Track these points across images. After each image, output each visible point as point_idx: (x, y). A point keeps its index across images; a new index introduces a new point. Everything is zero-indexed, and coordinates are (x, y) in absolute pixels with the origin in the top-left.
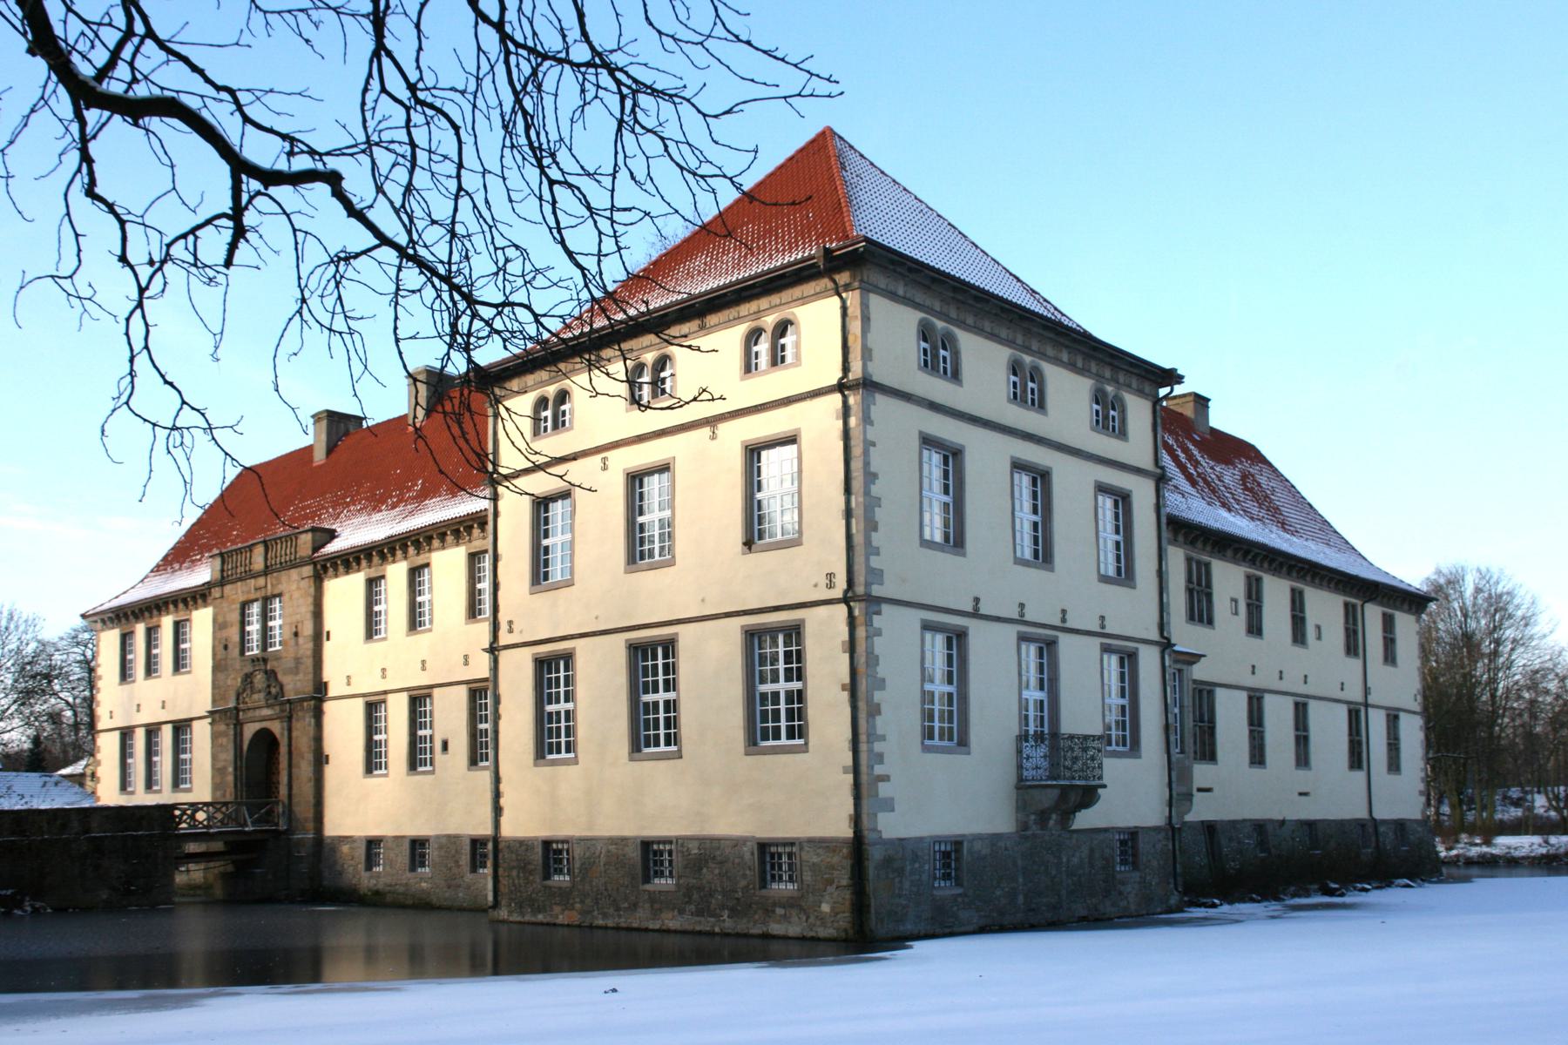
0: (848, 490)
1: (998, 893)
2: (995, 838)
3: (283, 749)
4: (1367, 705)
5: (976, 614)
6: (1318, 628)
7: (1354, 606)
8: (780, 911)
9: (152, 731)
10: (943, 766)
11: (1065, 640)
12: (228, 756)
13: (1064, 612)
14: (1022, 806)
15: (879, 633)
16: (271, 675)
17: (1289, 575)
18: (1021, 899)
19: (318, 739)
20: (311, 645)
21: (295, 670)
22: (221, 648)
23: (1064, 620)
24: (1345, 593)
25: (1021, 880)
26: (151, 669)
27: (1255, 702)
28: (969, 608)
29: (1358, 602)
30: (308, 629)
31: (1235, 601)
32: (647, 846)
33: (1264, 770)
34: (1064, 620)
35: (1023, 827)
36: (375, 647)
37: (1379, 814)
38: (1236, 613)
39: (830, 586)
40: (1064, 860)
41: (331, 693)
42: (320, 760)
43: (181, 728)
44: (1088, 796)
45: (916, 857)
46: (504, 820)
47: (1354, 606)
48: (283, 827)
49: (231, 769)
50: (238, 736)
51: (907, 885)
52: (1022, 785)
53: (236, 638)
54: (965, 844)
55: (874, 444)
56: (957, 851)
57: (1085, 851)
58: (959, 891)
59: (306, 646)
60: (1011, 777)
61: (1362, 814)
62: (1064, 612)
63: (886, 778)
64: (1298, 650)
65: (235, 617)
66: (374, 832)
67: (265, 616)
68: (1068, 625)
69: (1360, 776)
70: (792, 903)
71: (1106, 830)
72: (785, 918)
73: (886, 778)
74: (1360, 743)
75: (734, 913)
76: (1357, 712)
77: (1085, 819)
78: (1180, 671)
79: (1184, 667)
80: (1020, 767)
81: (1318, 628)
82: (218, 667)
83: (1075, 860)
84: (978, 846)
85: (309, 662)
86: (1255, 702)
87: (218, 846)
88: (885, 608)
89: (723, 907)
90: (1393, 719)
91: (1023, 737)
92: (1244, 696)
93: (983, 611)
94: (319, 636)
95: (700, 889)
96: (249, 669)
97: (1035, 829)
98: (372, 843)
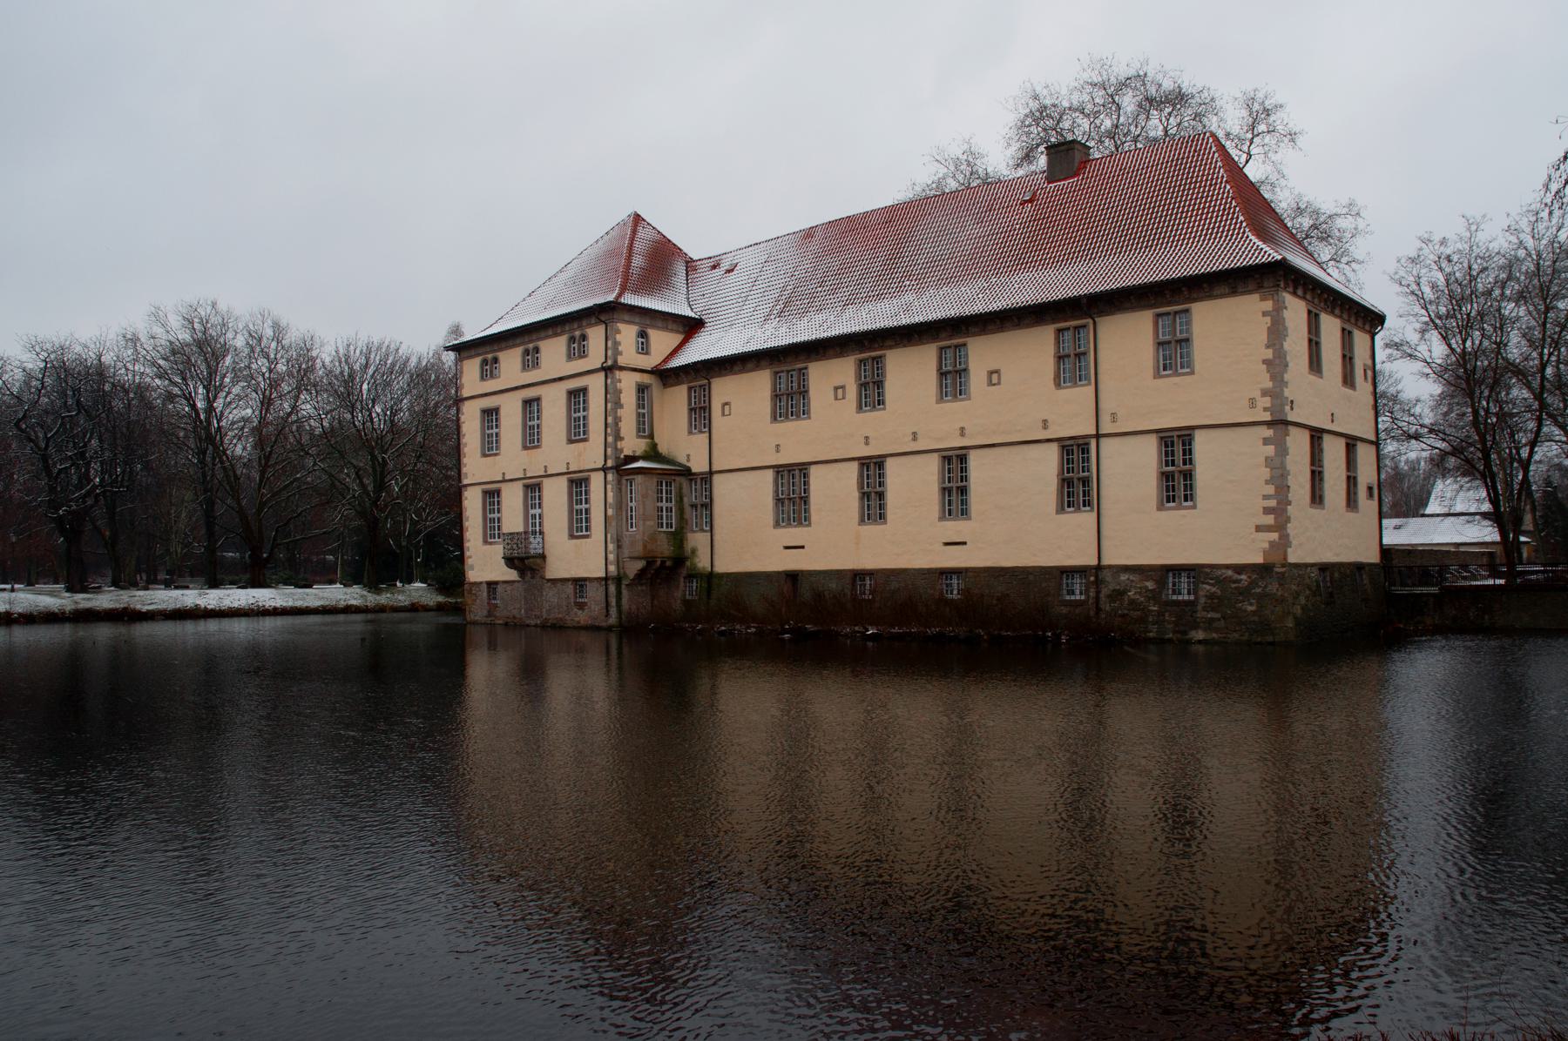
5: (504, 481)
13: (546, 467)
17: (935, 338)
23: (546, 471)
24: (1054, 321)
27: (872, 468)
28: (501, 479)
31: (843, 387)
33: (882, 527)
34: (546, 471)
37: (1110, 559)
62: (546, 467)
68: (549, 473)
69: (1087, 518)
76: (1085, 449)
79: (635, 477)
86: (872, 468)
88: (469, 488)
93: (507, 478)
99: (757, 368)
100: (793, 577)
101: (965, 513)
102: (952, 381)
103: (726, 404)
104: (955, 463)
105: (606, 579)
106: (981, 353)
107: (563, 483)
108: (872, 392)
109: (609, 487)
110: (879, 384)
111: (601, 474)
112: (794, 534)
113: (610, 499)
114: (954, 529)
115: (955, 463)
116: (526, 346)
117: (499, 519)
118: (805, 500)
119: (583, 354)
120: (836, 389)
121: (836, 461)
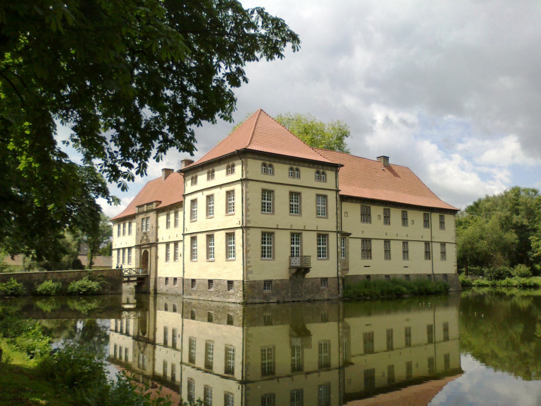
0: (242, 203)
1: (283, 292)
2: (281, 280)
3: (149, 255)
4: (432, 242)
6: (413, 221)
7: (428, 214)
8: (231, 296)
9: (124, 249)
10: (267, 263)
11: (304, 234)
12: (138, 256)
13: (305, 226)
14: (290, 272)
15: (249, 234)
16: (147, 236)
18: (290, 294)
19: (156, 253)
20: (155, 230)
21: (152, 236)
22: (138, 230)
23: (305, 228)
25: (290, 290)
26: (124, 234)
27: (387, 242)
29: (430, 213)
30: (155, 226)
31: (380, 216)
32: (210, 282)
34: (305, 228)
35: (291, 278)
36: (168, 230)
37: (435, 272)
38: (380, 219)
39: (240, 224)
40: (304, 285)
41: (160, 242)
42: (157, 258)
43: (130, 249)
44: (307, 270)
45: (258, 284)
46: (185, 274)
47: (428, 214)
48: (148, 274)
49: (139, 260)
50: (141, 251)
51: (256, 291)
52: (291, 268)
53: (141, 227)
54: (273, 282)
55: (248, 192)
56: (272, 283)
57: (311, 283)
58: (272, 292)
59: (154, 229)
60: (287, 266)
61: (430, 272)
62: (305, 226)
63: (251, 267)
64: (405, 228)
65: (140, 222)
66: (167, 276)
67: (146, 222)
69: (429, 262)
70: (233, 294)
71: (317, 278)
72: (232, 298)
73: (251, 267)
74: (429, 252)
75: (224, 297)
76: (429, 244)
77: (308, 275)
78: (345, 238)
79: (346, 237)
80: (290, 263)
81: (413, 221)
82: (137, 234)
83: (307, 285)
84: (277, 282)
85: (155, 234)
86: (387, 242)
87: (135, 279)
88: (251, 229)
89: (222, 295)
90: (443, 244)
91: (292, 256)
92: (383, 241)
93: (279, 227)
94: (157, 227)
95: (218, 291)
96: (143, 235)
97: (295, 278)
98: (167, 279)
99: (357, 202)
100: (368, 277)
101: (408, 258)
102: (405, 220)
103: (346, 212)
104: (405, 243)
105: (338, 277)
106: (412, 215)
107: (314, 235)
108: (387, 219)
109: (338, 239)
110: (389, 217)
111: (335, 234)
112: (367, 262)
113: (339, 245)
114: (406, 263)
115: (405, 243)
116: (292, 166)
117: (234, 247)
118: (370, 250)
119: (325, 180)
120: (378, 216)
121: (379, 239)
